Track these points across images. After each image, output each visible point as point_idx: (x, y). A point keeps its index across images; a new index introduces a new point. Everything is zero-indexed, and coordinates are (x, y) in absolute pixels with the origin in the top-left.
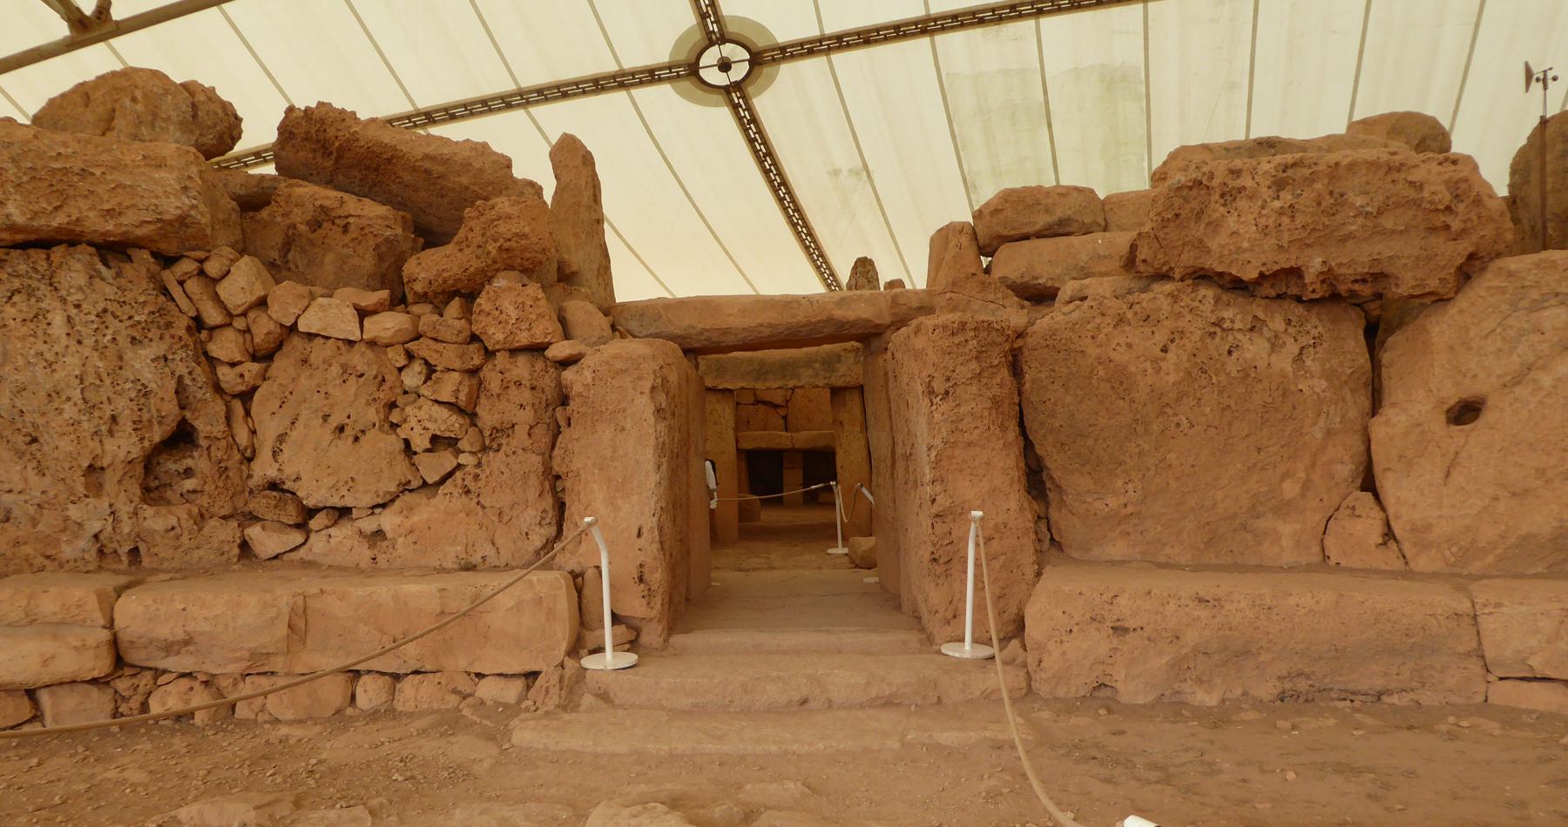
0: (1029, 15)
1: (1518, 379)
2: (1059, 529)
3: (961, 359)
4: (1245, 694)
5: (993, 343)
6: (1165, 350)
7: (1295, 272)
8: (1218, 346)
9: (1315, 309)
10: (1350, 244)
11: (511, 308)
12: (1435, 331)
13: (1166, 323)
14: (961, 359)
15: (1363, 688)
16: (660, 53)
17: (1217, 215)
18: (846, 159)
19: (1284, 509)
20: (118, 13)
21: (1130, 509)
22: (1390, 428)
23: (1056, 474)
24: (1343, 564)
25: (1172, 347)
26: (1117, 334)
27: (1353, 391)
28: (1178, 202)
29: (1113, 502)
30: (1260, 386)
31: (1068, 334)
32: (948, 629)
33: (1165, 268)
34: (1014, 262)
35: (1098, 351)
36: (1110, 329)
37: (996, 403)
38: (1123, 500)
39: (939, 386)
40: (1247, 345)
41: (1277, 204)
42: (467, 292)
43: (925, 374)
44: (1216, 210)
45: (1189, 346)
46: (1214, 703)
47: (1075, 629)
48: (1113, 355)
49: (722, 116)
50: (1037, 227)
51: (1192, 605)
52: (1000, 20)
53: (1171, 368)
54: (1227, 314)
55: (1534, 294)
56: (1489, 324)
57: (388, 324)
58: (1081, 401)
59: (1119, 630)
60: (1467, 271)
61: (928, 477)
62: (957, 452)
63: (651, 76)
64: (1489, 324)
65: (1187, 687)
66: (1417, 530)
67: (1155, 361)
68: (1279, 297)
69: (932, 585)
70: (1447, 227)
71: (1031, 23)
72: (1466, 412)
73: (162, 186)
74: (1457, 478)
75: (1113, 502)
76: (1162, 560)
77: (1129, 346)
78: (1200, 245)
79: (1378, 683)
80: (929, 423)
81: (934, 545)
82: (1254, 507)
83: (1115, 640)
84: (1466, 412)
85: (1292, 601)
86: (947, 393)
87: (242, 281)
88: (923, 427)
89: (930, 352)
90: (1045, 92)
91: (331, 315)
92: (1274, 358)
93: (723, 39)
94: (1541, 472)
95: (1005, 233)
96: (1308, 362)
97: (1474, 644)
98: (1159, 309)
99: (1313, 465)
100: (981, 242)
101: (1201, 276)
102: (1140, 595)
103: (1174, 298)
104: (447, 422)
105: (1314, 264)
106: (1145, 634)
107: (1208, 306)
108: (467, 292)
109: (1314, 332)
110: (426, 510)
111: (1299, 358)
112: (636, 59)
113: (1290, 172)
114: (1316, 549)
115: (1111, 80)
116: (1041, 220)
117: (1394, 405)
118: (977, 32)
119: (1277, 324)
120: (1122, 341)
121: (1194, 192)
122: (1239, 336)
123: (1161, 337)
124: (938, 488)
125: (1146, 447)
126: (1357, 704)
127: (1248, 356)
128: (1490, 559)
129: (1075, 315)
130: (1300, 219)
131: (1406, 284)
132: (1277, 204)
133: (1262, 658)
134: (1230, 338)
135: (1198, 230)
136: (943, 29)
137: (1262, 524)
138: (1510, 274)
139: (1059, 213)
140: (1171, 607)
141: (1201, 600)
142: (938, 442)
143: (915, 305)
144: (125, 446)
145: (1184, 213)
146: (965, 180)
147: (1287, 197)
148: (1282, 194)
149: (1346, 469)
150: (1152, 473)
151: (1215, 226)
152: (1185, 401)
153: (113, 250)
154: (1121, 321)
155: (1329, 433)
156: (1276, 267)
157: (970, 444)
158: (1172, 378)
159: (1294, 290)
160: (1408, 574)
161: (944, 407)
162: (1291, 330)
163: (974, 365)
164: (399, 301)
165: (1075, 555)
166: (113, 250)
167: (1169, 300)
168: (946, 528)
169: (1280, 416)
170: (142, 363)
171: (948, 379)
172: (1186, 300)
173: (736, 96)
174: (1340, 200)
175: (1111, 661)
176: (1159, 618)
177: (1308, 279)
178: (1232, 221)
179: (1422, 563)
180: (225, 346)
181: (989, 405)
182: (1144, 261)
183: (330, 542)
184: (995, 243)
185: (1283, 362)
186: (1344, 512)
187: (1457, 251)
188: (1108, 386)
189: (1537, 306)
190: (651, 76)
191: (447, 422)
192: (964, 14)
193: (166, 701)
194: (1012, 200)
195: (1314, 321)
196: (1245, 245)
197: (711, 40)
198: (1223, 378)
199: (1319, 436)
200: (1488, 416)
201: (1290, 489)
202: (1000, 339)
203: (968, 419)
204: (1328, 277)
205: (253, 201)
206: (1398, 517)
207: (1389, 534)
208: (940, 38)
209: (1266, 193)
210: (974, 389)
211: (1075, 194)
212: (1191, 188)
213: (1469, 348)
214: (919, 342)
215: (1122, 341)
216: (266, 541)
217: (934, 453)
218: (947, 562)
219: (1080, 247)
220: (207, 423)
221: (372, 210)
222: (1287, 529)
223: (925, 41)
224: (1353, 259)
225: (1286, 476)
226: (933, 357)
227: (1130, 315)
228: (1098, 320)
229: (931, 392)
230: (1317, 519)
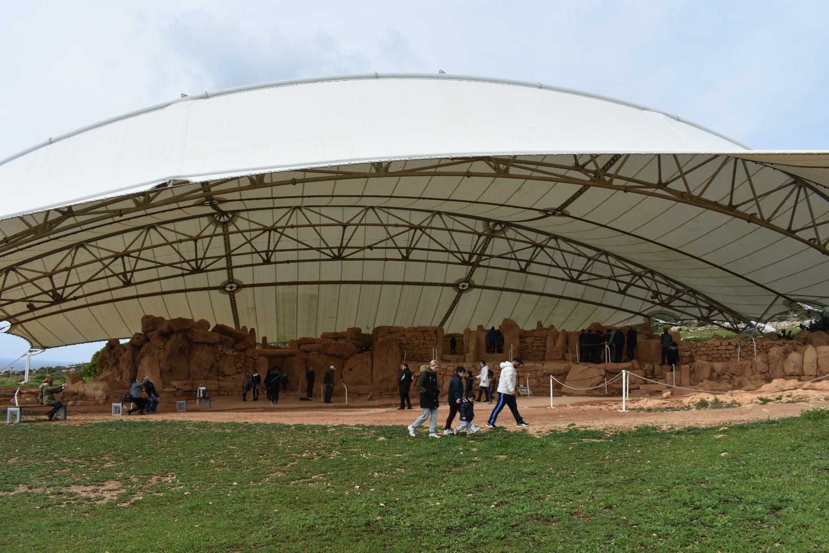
22: (344, 371)
34: (302, 347)
42: (244, 350)
49: (227, 297)
57: (236, 354)
60: (352, 355)
63: (215, 288)
84: (351, 369)
91: (230, 352)
104: (242, 365)
108: (244, 350)
110: (240, 376)
112: (212, 285)
115: (311, 297)
144: (208, 367)
153: (208, 344)
166: (208, 344)
173: (232, 295)
183: (227, 379)
190: (215, 288)
191: (242, 365)
193: (222, 393)
197: (230, 283)
218: (298, 383)
219: (312, 346)
221: (231, 339)
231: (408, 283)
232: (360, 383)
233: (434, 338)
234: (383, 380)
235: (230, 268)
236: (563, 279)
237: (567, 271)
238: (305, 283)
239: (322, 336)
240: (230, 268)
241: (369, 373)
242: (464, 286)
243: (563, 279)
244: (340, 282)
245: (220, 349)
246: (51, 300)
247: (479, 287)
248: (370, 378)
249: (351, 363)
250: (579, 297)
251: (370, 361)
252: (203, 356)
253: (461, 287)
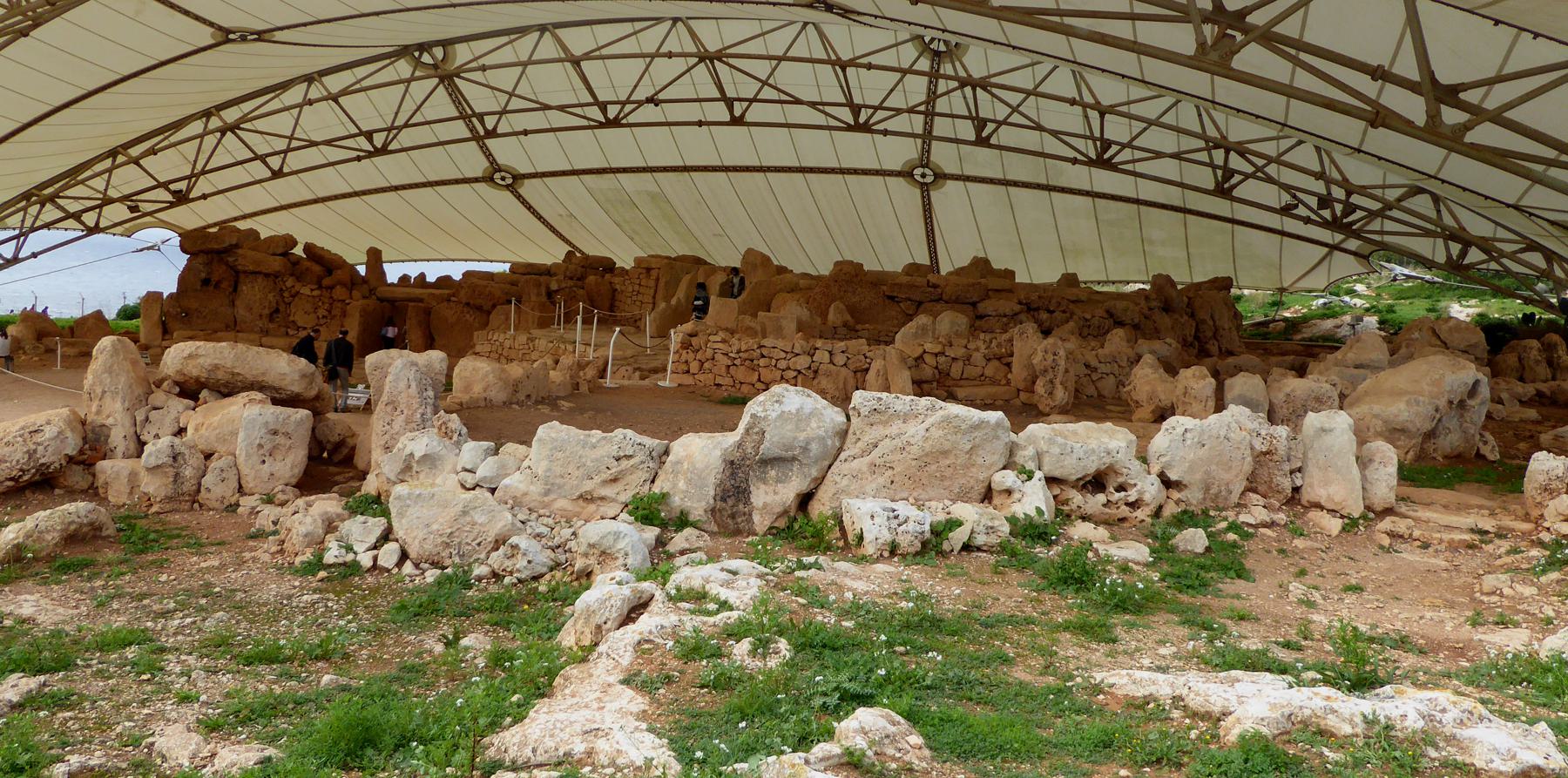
11: (339, 292)
16: (479, 174)
18: (562, 211)
20: (286, 170)
26: (448, 313)
42: (331, 288)
57: (316, 293)
60: (494, 306)
63: (476, 180)
73: (276, 264)
87: (289, 283)
91: (306, 291)
93: (500, 170)
108: (331, 288)
115: (653, 197)
144: (267, 312)
153: (267, 275)
164: (320, 287)
170: (270, 296)
180: (286, 294)
190: (476, 180)
205: (298, 260)
216: (291, 332)
220: (282, 308)
221: (317, 269)
224: (479, 302)
233: (652, 283)
235: (927, 136)
240: (927, 136)
242: (924, 176)
245: (289, 283)
246: (170, 198)
252: (254, 295)
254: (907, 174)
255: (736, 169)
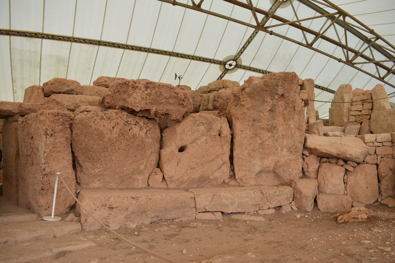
0: (40, 38)
1: (194, 141)
2: (80, 179)
3: (57, 124)
4: (142, 223)
5: (67, 121)
6: (113, 128)
7: (148, 111)
8: (127, 128)
9: (150, 121)
10: (162, 105)
12: (177, 129)
13: (114, 120)
14: (57, 124)
15: (169, 218)
17: (130, 93)
19: (140, 172)
21: (101, 173)
23: (81, 162)
24: (153, 186)
25: (115, 127)
27: (157, 142)
28: (119, 88)
29: (97, 171)
30: (137, 140)
31: (87, 120)
32: (46, 212)
33: (113, 105)
35: (95, 126)
36: (99, 120)
37: (67, 138)
38: (99, 170)
39: (49, 132)
40: (134, 129)
41: (147, 92)
43: (44, 128)
44: (131, 91)
45: (120, 127)
46: (135, 227)
47: (97, 209)
48: (99, 128)
50: (64, 91)
51: (131, 199)
52: (32, 36)
53: (115, 133)
54: (130, 120)
55: (198, 122)
56: (189, 128)
58: (90, 141)
59: (111, 208)
61: (43, 162)
62: (54, 154)
64: (189, 128)
65: (128, 223)
66: (171, 177)
67: (111, 131)
68: (142, 117)
69: (41, 198)
70: (183, 104)
71: (40, 40)
72: (182, 149)
74: (180, 165)
75: (97, 171)
76: (109, 187)
77: (104, 126)
78: (125, 100)
79: (174, 217)
80: (45, 144)
81: (43, 184)
82: (133, 172)
83: (110, 211)
84: (182, 149)
85: (155, 197)
86: (52, 135)
88: (43, 145)
89: (47, 121)
90: (41, 59)
92: (140, 132)
94: (197, 163)
95: (54, 90)
96: (148, 134)
97: (194, 205)
98: (113, 116)
99: (147, 161)
100: (45, 92)
101: (123, 109)
102: (117, 198)
103: (117, 114)
105: (153, 109)
106: (118, 209)
107: (125, 117)
109: (150, 127)
111: (146, 133)
113: (148, 85)
114: (146, 183)
115: (59, 60)
116: (65, 89)
117: (167, 146)
118: (24, 38)
119: (142, 124)
120: (102, 124)
121: (124, 86)
122: (132, 126)
123: (113, 124)
124: (46, 166)
125: (107, 155)
126: (169, 222)
127: (134, 131)
128: (186, 184)
129: (89, 115)
130: (151, 97)
131: (174, 116)
132: (147, 92)
133: (148, 213)
134: (130, 126)
135: (125, 96)
136: (14, 35)
137: (134, 177)
138: (194, 117)
139: (71, 88)
140: (125, 201)
141: (133, 198)
142: (48, 150)
143: (27, 107)
145: (121, 91)
146: (12, 79)
147: (149, 91)
148: (148, 90)
149: (154, 163)
150: (108, 162)
151: (129, 95)
152: (117, 143)
154: (102, 118)
155: (152, 153)
156: (145, 109)
157: (59, 152)
158: (115, 136)
159: (147, 115)
160: (168, 189)
161: (51, 139)
162: (145, 126)
163: (61, 127)
165: (84, 186)
167: (115, 114)
168: (48, 179)
169: (141, 148)
171: (53, 130)
172: (120, 115)
174: (161, 94)
175: (109, 218)
176: (122, 204)
177: (152, 113)
178: (135, 94)
179: (171, 186)
181: (65, 140)
182: (108, 103)
184: (50, 93)
185: (142, 134)
186: (153, 173)
187: (184, 110)
188: (97, 137)
189: (198, 125)
192: (21, 32)
194: (57, 81)
195: (150, 124)
196: (138, 101)
198: (128, 137)
199: (149, 153)
200: (187, 150)
201: (142, 167)
202: (69, 120)
203: (58, 144)
204: (156, 113)
206: (166, 174)
207: (164, 178)
208: (12, 37)
209: (143, 89)
210: (61, 134)
211: (76, 83)
212: (123, 84)
213: (184, 134)
214: (42, 118)
215: (102, 124)
217: (46, 154)
218: (47, 189)
219: (77, 98)
222: (140, 178)
223: (8, 37)
224: (162, 109)
225: (142, 164)
226: (48, 123)
227: (105, 117)
228: (96, 117)
229: (46, 134)
230: (147, 175)
231: (177, 55)
232: (203, 182)
234: (260, 172)
236: (340, 61)
237: (345, 50)
238: (53, 37)
239: (98, 83)
241: (226, 158)
242: (230, 65)
243: (340, 61)
244: (99, 43)
247: (245, 68)
248: (226, 168)
249: (184, 132)
250: (325, 86)
251: (226, 131)
253: (227, 66)
254: (222, 63)
255: (133, 48)
